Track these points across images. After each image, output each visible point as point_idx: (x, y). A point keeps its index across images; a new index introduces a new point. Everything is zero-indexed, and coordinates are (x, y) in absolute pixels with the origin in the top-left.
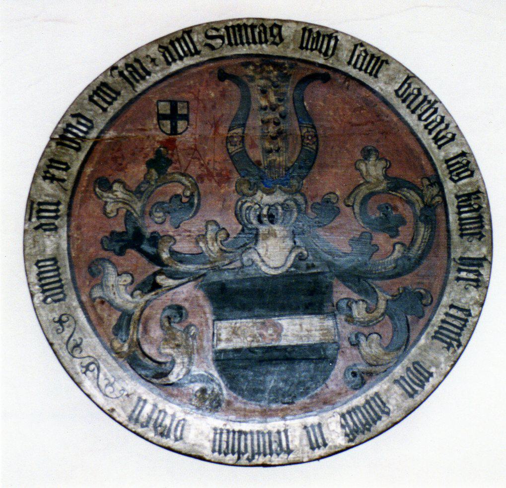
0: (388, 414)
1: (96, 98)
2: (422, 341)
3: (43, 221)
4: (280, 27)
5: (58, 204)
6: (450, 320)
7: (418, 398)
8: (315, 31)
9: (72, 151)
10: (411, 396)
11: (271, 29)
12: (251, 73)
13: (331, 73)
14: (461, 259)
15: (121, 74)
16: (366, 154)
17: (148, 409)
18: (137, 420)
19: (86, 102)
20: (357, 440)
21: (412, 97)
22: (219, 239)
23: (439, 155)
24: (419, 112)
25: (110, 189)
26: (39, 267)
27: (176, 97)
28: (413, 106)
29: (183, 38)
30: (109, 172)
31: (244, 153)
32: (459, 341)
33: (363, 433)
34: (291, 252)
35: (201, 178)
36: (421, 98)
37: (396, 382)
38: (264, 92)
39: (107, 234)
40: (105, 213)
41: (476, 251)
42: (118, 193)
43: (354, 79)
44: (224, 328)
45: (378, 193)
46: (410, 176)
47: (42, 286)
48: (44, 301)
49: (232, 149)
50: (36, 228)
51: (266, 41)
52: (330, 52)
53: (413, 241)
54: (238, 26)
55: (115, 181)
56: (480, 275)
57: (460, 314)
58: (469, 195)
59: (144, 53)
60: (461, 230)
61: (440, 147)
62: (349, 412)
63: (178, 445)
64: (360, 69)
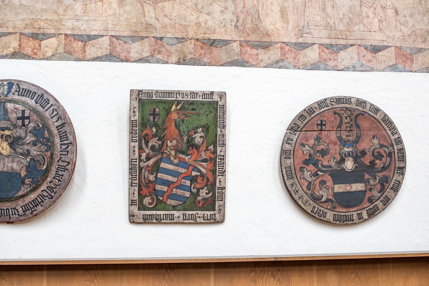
0: (379, 210)
1: (300, 119)
2: (388, 190)
3: (287, 156)
4: (351, 99)
5: (290, 151)
6: (395, 184)
7: (386, 205)
8: (360, 100)
9: (294, 135)
10: (385, 205)
11: (348, 100)
12: (343, 113)
13: (365, 114)
14: (398, 167)
15: (307, 112)
16: (374, 137)
17: (316, 209)
18: (313, 212)
19: (297, 120)
20: (371, 217)
21: (386, 121)
22: (334, 161)
23: (393, 138)
24: (387, 125)
25: (304, 146)
26: (286, 169)
27: (322, 119)
28: (386, 124)
29: (324, 101)
30: (304, 141)
31: (341, 136)
32: (397, 190)
33: (372, 215)
34: (354, 165)
35: (329, 143)
36: (388, 121)
37: (381, 201)
38: (346, 118)
39: (304, 160)
40: (303, 154)
41: (402, 165)
42: (307, 148)
43: (370, 115)
44: (336, 187)
45: (377, 148)
46: (385, 144)
47: (287, 175)
48: (288, 179)
49: (337, 135)
50: (285, 158)
51: (347, 103)
52: (364, 107)
53: (386, 162)
54: (339, 98)
55: (306, 144)
56: (403, 171)
57: (398, 183)
58: (400, 149)
59: (313, 106)
60: (398, 159)
61: (393, 135)
62: (369, 210)
63: (324, 219)
64: (372, 112)
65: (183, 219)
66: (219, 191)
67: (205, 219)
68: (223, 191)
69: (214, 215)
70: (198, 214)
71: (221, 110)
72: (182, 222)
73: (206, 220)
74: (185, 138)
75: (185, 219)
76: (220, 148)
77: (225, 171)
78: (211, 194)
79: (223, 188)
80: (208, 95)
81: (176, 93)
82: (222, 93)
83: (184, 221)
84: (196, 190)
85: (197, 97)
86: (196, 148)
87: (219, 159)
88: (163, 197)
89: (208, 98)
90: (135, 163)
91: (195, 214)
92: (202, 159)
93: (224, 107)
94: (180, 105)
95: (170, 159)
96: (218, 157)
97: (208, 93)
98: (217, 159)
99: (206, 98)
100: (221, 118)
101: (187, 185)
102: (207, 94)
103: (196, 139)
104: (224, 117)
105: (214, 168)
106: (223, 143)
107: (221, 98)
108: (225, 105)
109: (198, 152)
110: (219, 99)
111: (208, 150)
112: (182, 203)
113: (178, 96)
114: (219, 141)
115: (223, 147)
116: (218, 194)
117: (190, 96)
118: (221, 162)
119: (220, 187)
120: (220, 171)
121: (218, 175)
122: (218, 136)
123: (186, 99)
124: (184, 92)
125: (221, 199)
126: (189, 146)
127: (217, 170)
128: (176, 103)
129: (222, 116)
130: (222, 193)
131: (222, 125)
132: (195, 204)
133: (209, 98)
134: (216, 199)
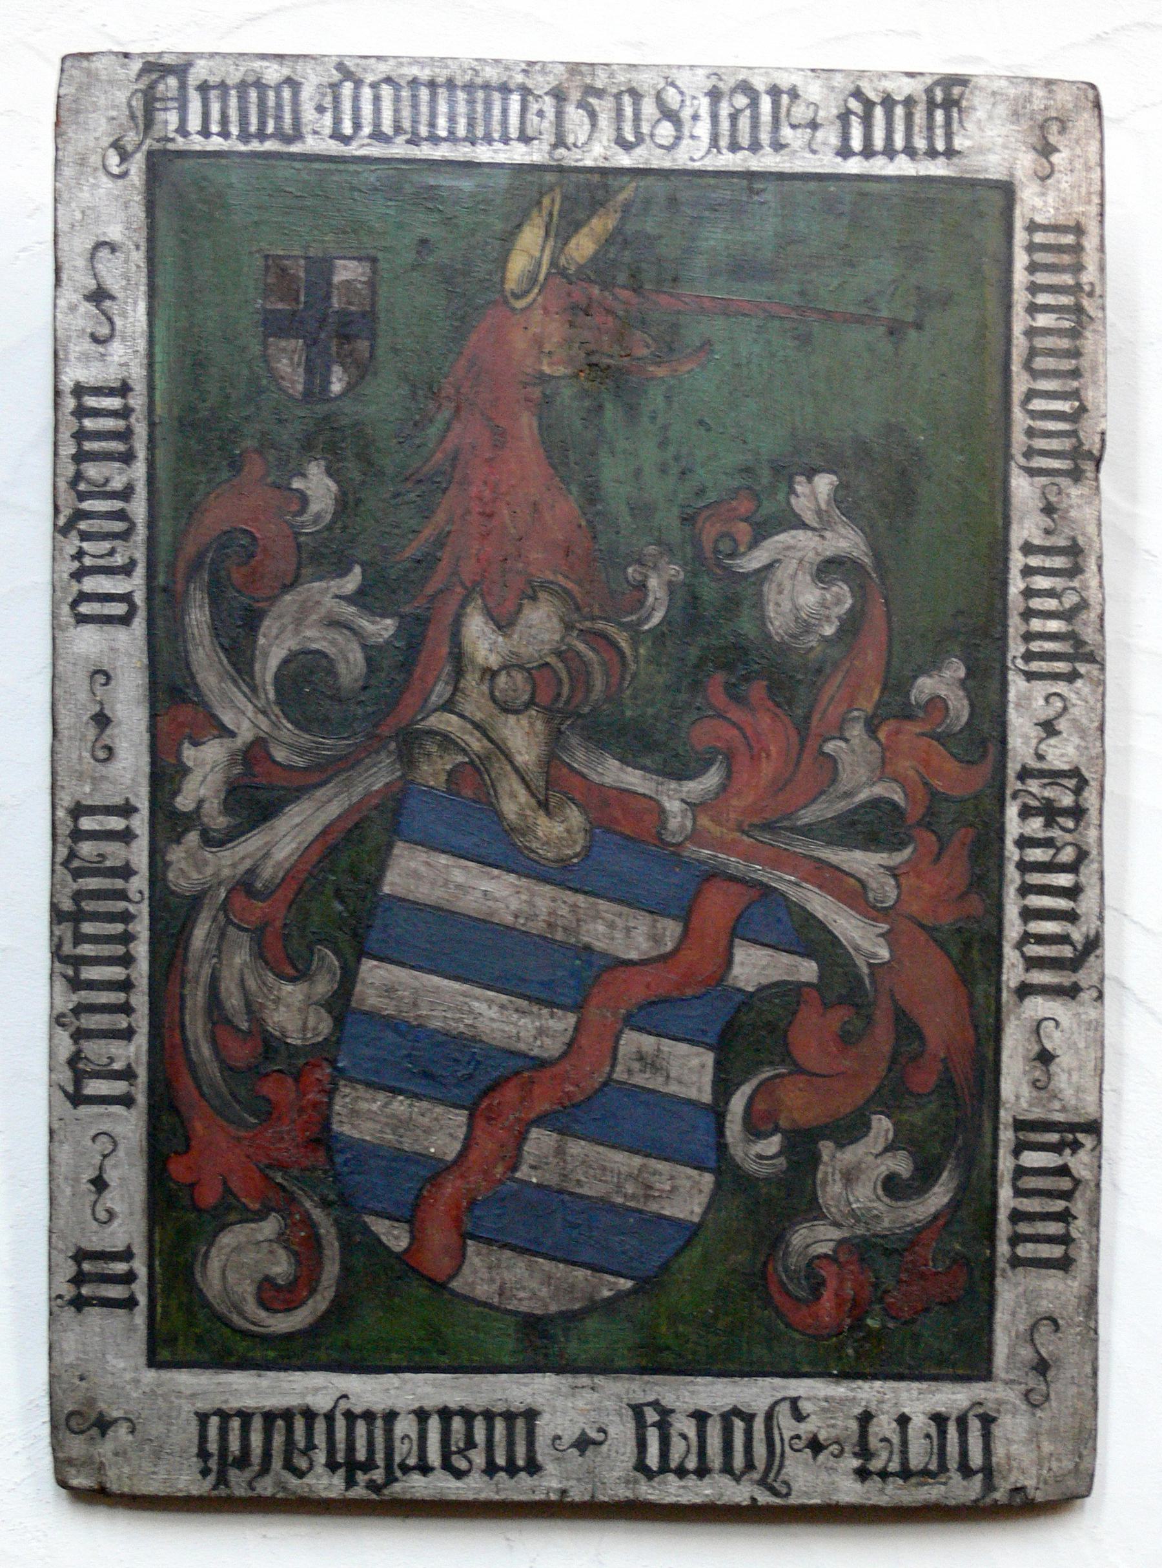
65: (641, 1466)
66: (1032, 1159)
67: (876, 1465)
68: (1079, 1163)
69: (975, 1426)
70: (799, 1416)
71: (1042, 278)
72: (623, 1493)
73: (884, 1474)
74: (653, 582)
75: (653, 1460)
76: (1041, 688)
77: (1094, 944)
78: (938, 1197)
79: (1073, 1127)
80: (909, 117)
81: (559, 95)
82: (1064, 97)
83: (648, 1492)
84: (772, 1145)
85: (786, 133)
86: (774, 689)
87: (1026, 813)
88: (412, 1218)
89: (899, 142)
90: (115, 853)
91: (770, 1416)
92: (842, 806)
93: (1078, 249)
94: (601, 224)
95: (488, 805)
96: (1013, 784)
97: (902, 88)
98: (1012, 811)
99: (879, 142)
100: (1050, 363)
101: (673, 1088)
102: (888, 102)
103: (770, 591)
104: (1076, 354)
105: (975, 904)
106: (1071, 637)
107: (1046, 150)
108: (1092, 227)
109: (803, 727)
110: (1025, 162)
111: (907, 713)
112: (626, 1284)
113: (575, 116)
114: (1028, 614)
115: (1072, 677)
116: (1019, 1192)
117: (703, 129)
118: (1048, 843)
119: (1036, 1114)
120: (1041, 939)
121: (1025, 991)
122: (1017, 560)
123: (660, 161)
124: (646, 81)
125: (1057, 1251)
126: (702, 660)
127: (1013, 928)
128: (552, 203)
129: (1064, 343)
130: (1065, 1184)
131: (1055, 444)
132: (768, 1302)
133: (920, 144)
134: (1003, 1248)
